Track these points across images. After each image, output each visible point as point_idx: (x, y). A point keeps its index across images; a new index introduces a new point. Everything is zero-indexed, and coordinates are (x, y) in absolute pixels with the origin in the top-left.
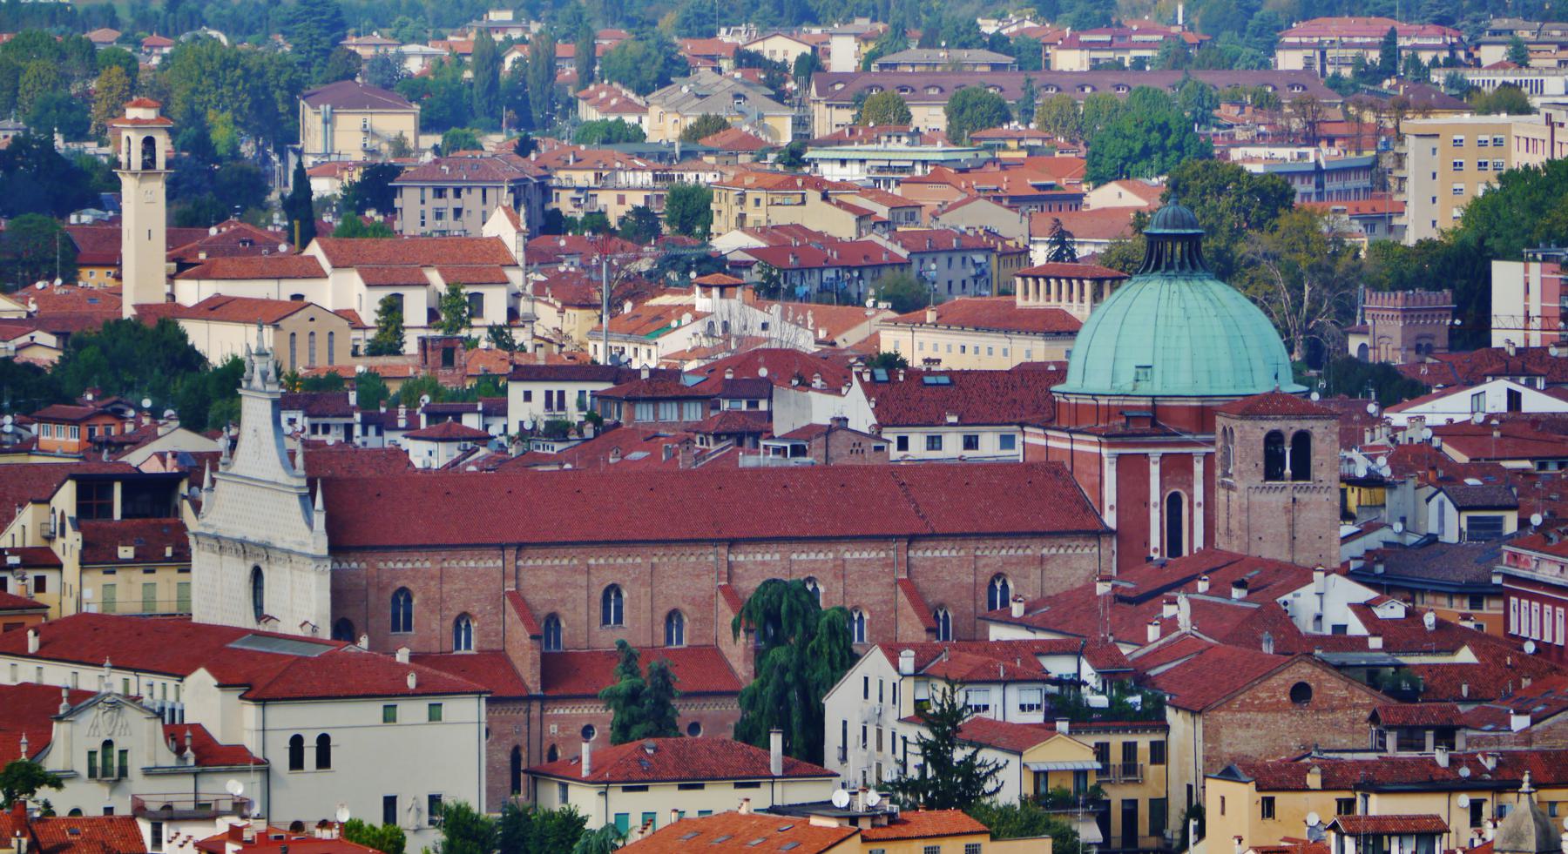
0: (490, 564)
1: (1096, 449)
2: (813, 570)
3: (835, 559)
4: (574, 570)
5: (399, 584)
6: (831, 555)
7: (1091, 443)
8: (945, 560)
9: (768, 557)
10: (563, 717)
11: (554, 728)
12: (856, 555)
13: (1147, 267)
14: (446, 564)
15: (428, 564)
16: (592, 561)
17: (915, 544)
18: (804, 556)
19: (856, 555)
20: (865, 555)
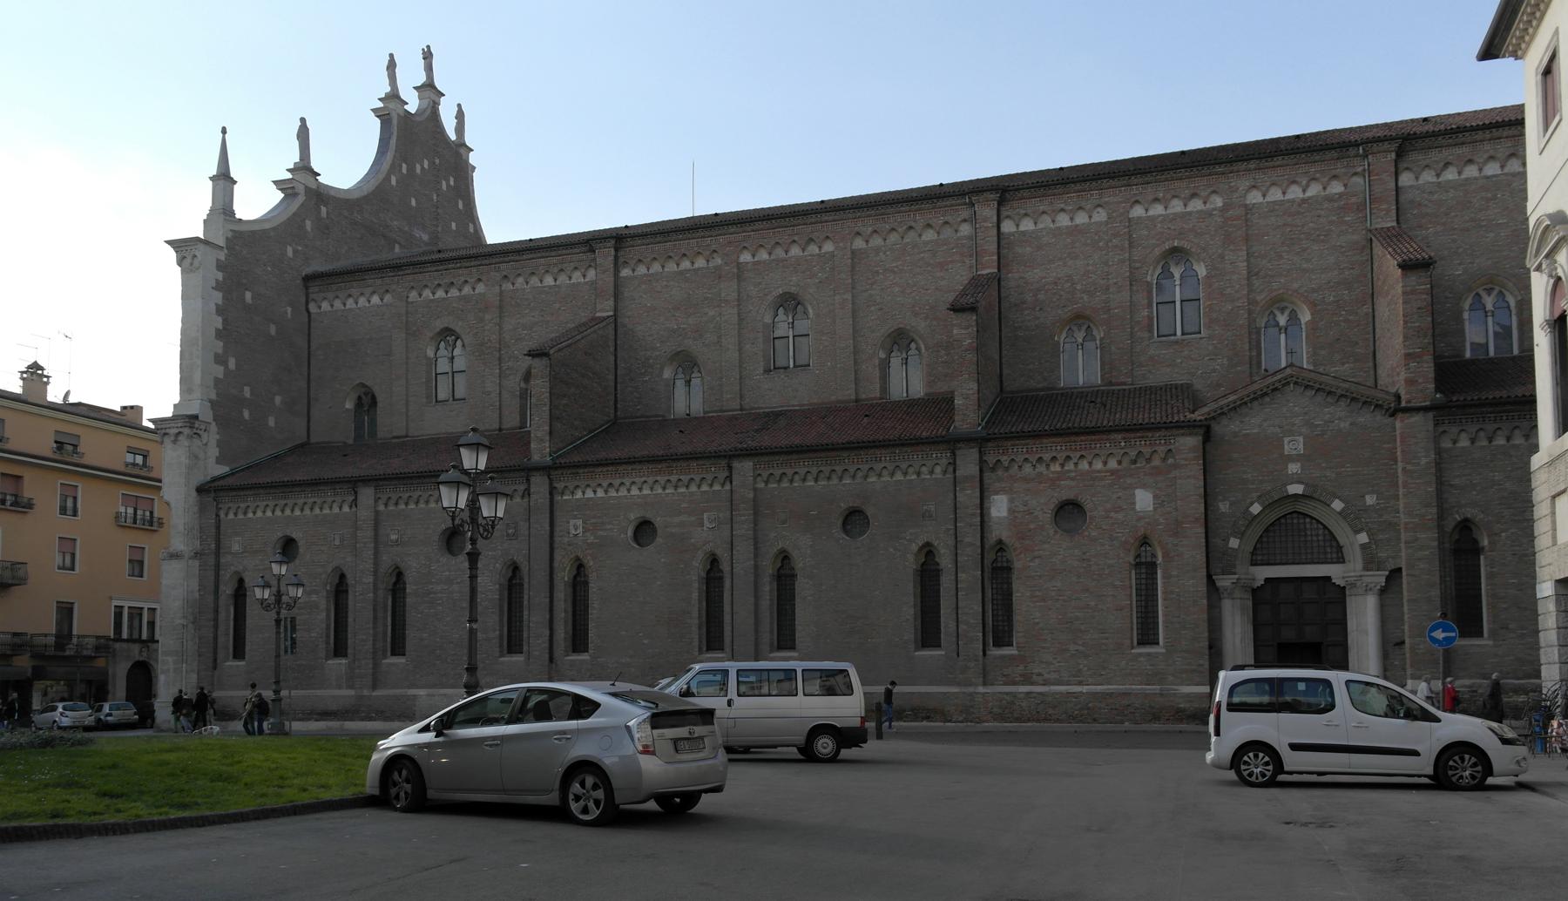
0: (577, 277)
5: (439, 325)
6: (1218, 201)
9: (1081, 218)
12: (1275, 195)
14: (507, 286)
15: (480, 288)
16: (746, 257)
17: (1414, 157)
18: (1158, 210)
20: (1295, 193)
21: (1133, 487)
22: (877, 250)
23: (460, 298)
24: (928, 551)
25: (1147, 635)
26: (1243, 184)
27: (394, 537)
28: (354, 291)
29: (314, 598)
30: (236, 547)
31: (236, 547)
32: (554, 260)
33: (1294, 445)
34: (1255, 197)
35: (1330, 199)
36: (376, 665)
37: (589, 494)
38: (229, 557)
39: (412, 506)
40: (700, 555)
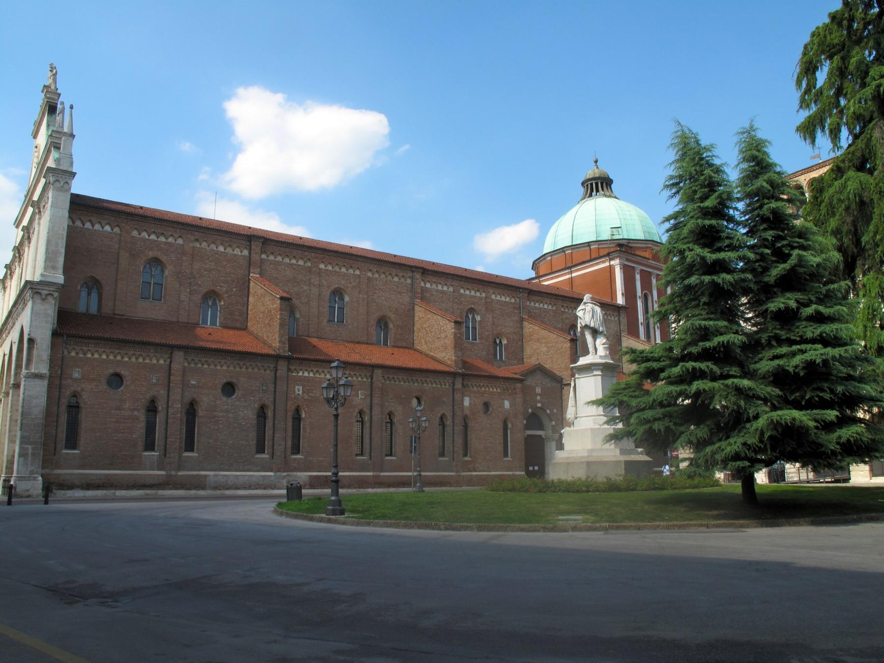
0: (237, 252)
1: (607, 264)
2: (473, 303)
3: (486, 298)
4: (309, 270)
5: (151, 254)
7: (603, 262)
8: (545, 311)
9: (445, 288)
10: (308, 379)
11: (299, 390)
12: (498, 298)
13: (592, 191)
16: (322, 266)
18: (467, 292)
19: (498, 298)
20: (503, 299)
21: (503, 399)
22: (376, 279)
23: (166, 243)
24: (442, 418)
25: (506, 455)
26: (491, 291)
27: (193, 382)
28: (93, 219)
29: (136, 413)
30: (76, 375)
31: (76, 375)
32: (227, 239)
33: (538, 390)
34: (493, 297)
35: (511, 303)
36: (180, 456)
37: (306, 374)
38: (70, 381)
39: (206, 366)
40: (357, 410)
